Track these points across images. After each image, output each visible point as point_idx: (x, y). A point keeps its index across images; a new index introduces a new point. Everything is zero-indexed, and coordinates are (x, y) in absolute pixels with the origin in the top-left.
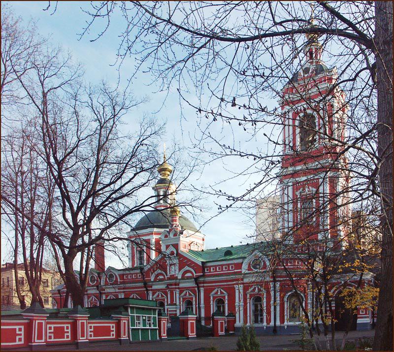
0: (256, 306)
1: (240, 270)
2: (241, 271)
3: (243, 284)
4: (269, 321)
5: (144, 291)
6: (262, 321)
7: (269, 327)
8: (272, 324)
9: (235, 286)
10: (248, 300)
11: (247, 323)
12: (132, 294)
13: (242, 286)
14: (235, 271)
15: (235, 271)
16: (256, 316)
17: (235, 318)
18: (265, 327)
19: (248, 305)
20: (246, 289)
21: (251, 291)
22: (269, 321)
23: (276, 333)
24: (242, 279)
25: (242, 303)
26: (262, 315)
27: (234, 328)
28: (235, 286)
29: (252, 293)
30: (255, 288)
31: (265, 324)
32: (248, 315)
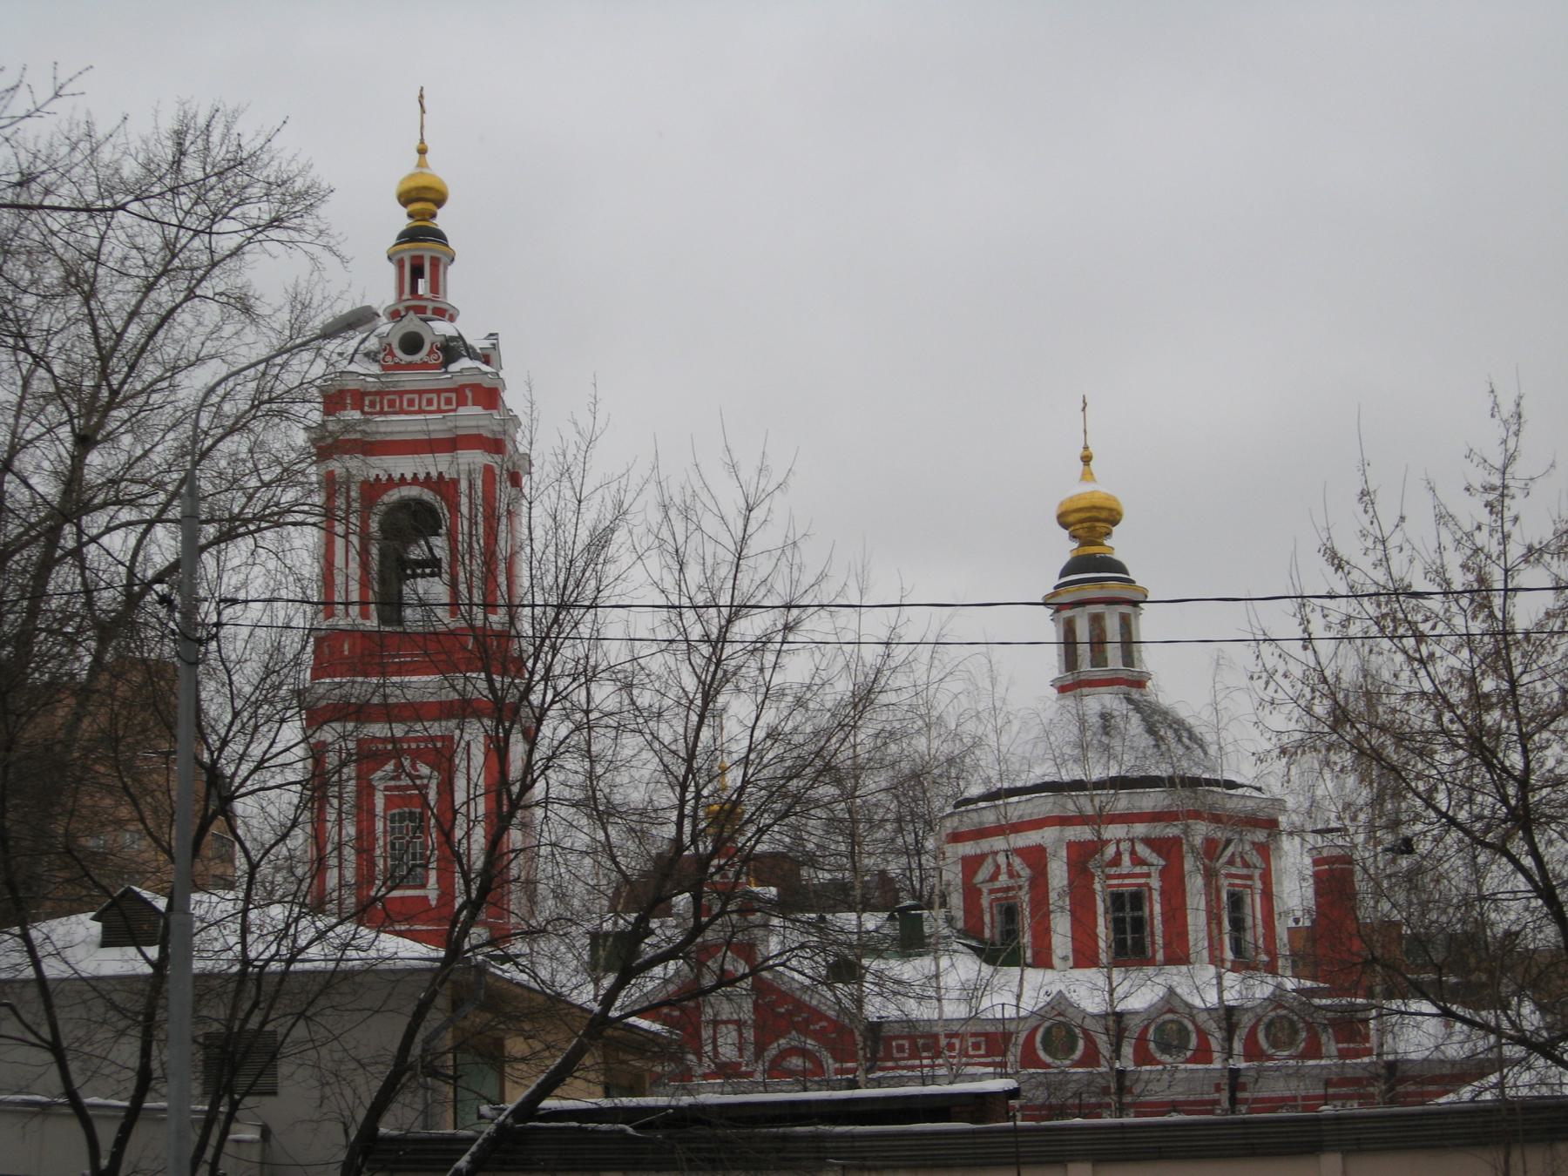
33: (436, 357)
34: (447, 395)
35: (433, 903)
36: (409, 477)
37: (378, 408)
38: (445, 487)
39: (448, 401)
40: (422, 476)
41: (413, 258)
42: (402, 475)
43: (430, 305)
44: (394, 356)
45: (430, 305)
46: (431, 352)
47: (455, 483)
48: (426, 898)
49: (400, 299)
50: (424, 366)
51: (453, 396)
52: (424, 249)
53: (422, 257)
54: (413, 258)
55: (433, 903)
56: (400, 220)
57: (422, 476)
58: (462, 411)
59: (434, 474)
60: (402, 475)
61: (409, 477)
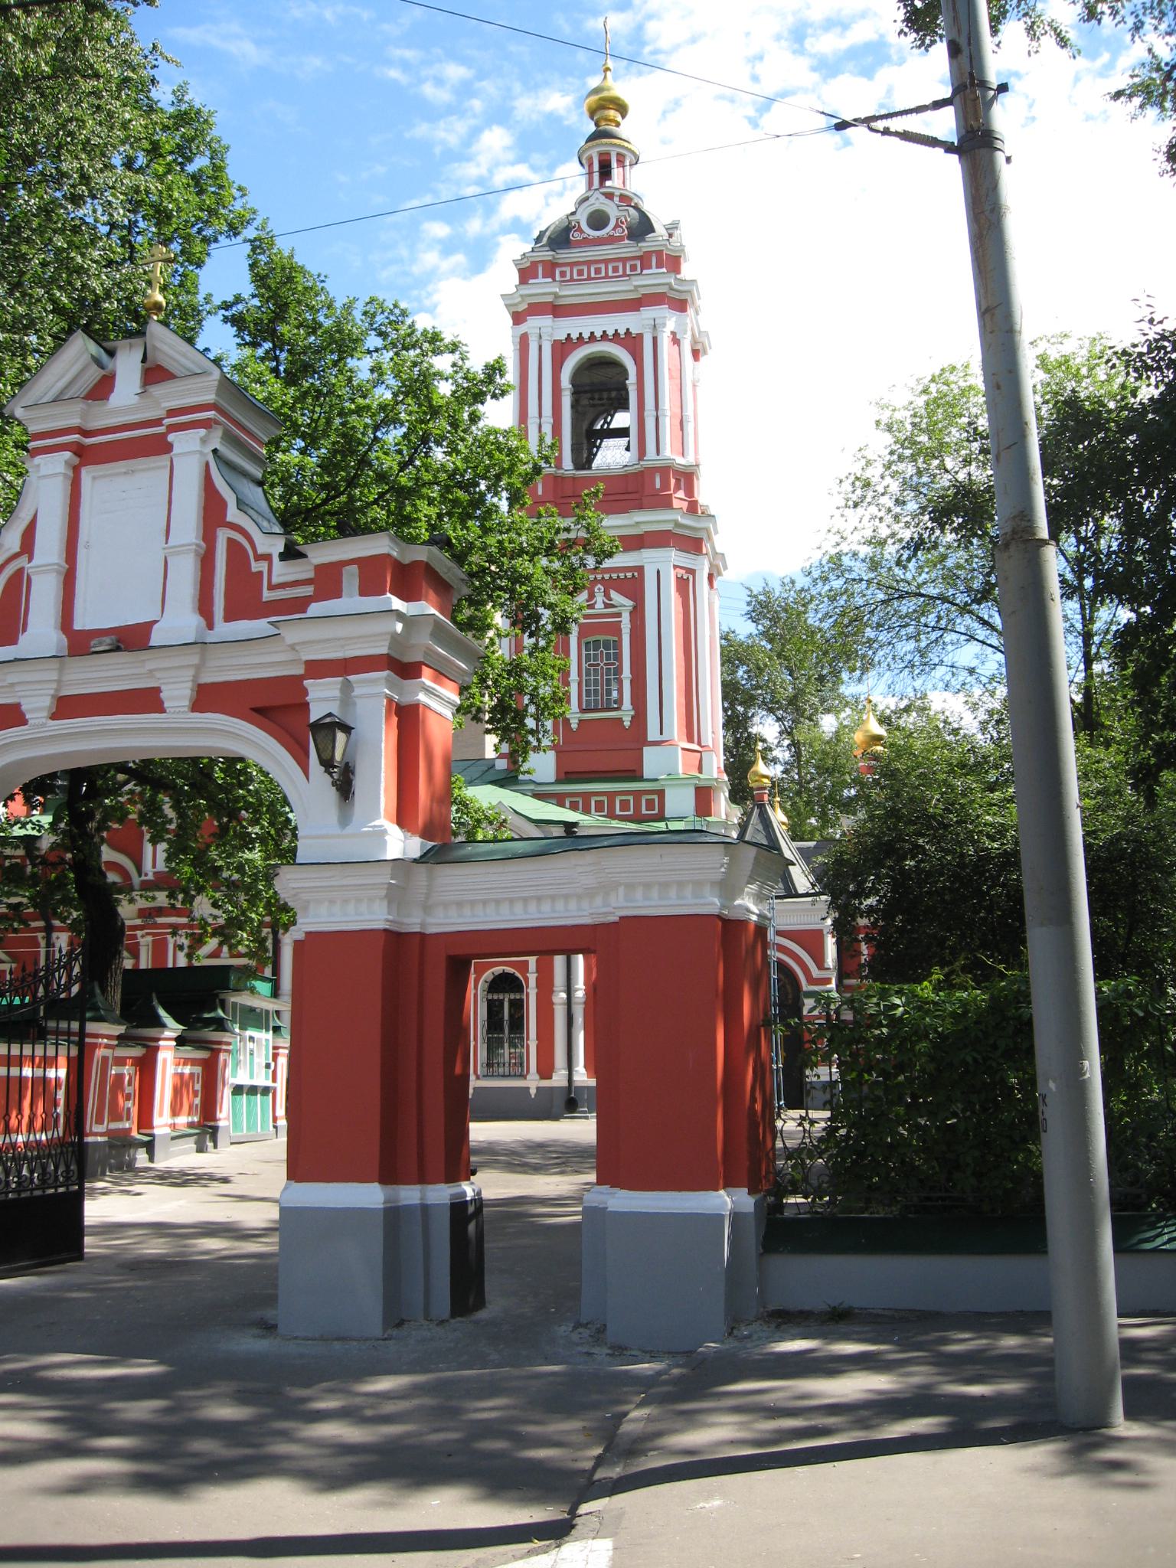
0: (494, 1009)
33: (621, 230)
34: (633, 263)
35: (627, 724)
36: (598, 334)
37: (568, 277)
38: (631, 342)
39: (634, 267)
40: (610, 333)
41: (601, 154)
42: (592, 333)
44: (582, 232)
45: (617, 193)
46: (617, 226)
47: (640, 336)
48: (620, 720)
50: (611, 240)
51: (638, 263)
52: (612, 145)
53: (608, 154)
54: (601, 154)
55: (627, 724)
57: (610, 333)
58: (645, 272)
59: (622, 331)
60: (592, 333)
61: (598, 334)
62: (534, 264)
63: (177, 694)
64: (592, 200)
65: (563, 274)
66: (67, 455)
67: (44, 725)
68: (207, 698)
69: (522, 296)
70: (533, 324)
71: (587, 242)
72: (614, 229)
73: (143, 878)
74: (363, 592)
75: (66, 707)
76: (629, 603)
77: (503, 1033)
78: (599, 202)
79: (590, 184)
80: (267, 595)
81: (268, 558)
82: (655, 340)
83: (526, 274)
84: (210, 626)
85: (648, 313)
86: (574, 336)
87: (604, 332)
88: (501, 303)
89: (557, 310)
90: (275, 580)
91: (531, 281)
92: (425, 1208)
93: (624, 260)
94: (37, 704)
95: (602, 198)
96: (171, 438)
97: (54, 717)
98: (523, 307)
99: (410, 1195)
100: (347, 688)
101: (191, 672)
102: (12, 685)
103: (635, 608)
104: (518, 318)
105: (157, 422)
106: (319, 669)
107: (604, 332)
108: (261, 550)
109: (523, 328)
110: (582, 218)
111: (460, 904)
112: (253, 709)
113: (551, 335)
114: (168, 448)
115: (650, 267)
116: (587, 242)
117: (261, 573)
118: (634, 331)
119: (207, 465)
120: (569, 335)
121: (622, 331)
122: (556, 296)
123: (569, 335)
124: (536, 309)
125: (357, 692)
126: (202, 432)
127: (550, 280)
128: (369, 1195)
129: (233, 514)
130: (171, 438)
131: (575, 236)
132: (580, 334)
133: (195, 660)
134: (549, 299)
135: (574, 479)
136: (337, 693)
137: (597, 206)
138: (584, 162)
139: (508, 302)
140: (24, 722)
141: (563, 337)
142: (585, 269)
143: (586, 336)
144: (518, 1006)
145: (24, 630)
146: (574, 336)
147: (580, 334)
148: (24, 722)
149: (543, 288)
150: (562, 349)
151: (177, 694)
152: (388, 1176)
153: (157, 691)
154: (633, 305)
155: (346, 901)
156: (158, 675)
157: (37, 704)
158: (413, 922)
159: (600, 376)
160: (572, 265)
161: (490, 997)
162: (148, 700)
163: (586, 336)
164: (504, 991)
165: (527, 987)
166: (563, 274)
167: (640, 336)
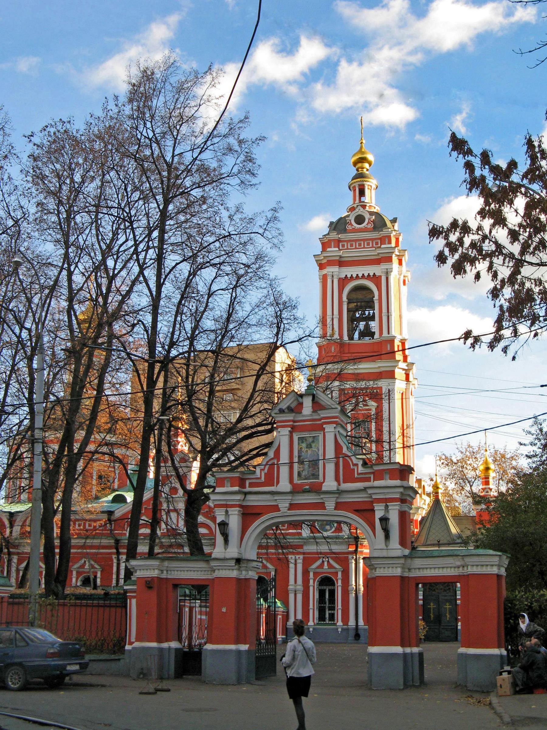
0: (322, 593)
1: (300, 531)
2: (300, 534)
3: (304, 553)
4: (345, 619)
5: (111, 553)
6: (332, 617)
7: (348, 629)
8: (352, 623)
9: (290, 557)
10: (311, 582)
11: (309, 621)
12: (81, 558)
13: (301, 557)
14: (291, 531)
15: (291, 531)
16: (322, 611)
17: (288, 612)
18: (340, 630)
19: (311, 589)
20: (307, 563)
21: (318, 567)
22: (345, 619)
23: (358, 639)
24: (301, 547)
25: (300, 587)
26: (332, 608)
27: (287, 628)
28: (290, 557)
29: (318, 570)
30: (323, 562)
31: (340, 623)
32: (311, 606)
36: (360, 275)
38: (376, 279)
39: (377, 244)
40: (366, 275)
42: (357, 275)
43: (368, 205)
44: (352, 225)
46: (368, 223)
47: (380, 276)
49: (354, 203)
50: (365, 230)
51: (379, 241)
56: (354, 172)
57: (366, 275)
58: (383, 246)
59: (371, 274)
60: (357, 275)
61: (360, 275)
62: (330, 241)
63: (330, 505)
64: (357, 210)
65: (343, 246)
66: (290, 429)
67: (286, 512)
68: (339, 506)
69: (324, 257)
70: (329, 270)
71: (354, 231)
72: (367, 224)
73: (162, 531)
74: (390, 479)
75: (292, 507)
76: (375, 404)
77: (325, 603)
78: (359, 211)
79: (355, 200)
80: (356, 476)
81: (357, 465)
82: (387, 279)
83: (325, 245)
84: (339, 484)
85: (384, 266)
86: (349, 276)
87: (363, 274)
88: (313, 260)
89: (341, 263)
90: (359, 472)
91: (328, 249)
92: (412, 654)
93: (372, 240)
94: (284, 505)
95: (362, 209)
96: (324, 426)
97: (289, 510)
98: (324, 261)
99: (408, 650)
100: (387, 507)
101: (335, 499)
102: (276, 500)
103: (378, 406)
104: (321, 266)
105: (320, 420)
106: (379, 501)
107: (363, 274)
108: (354, 462)
109: (324, 272)
110: (352, 219)
111: (419, 569)
112: (355, 510)
113: (338, 276)
114: (324, 429)
115: (385, 244)
116: (354, 231)
117: (354, 469)
118: (377, 274)
119: (335, 435)
120: (346, 275)
121: (371, 274)
122: (341, 257)
123: (346, 275)
124: (331, 263)
125: (390, 508)
126: (335, 425)
127: (337, 249)
128: (398, 650)
129: (345, 450)
130: (324, 426)
131: (349, 227)
132: (352, 275)
133: (337, 496)
134: (337, 258)
135: (349, 344)
136: (384, 508)
137: (360, 213)
138: (351, 188)
139: (317, 259)
140: (279, 511)
141: (343, 276)
142: (354, 243)
143: (354, 276)
144: (332, 593)
145: (278, 482)
146: (349, 276)
147: (352, 275)
148: (279, 511)
149: (333, 252)
150: (343, 282)
151: (330, 505)
152: (403, 646)
153: (324, 503)
154: (377, 262)
155: (389, 568)
156: (324, 499)
157: (284, 505)
158: (406, 574)
159: (359, 295)
160: (347, 241)
161: (320, 588)
162: (322, 506)
163: (354, 276)
164: (326, 585)
165: (337, 583)
166: (343, 246)
167: (380, 276)
